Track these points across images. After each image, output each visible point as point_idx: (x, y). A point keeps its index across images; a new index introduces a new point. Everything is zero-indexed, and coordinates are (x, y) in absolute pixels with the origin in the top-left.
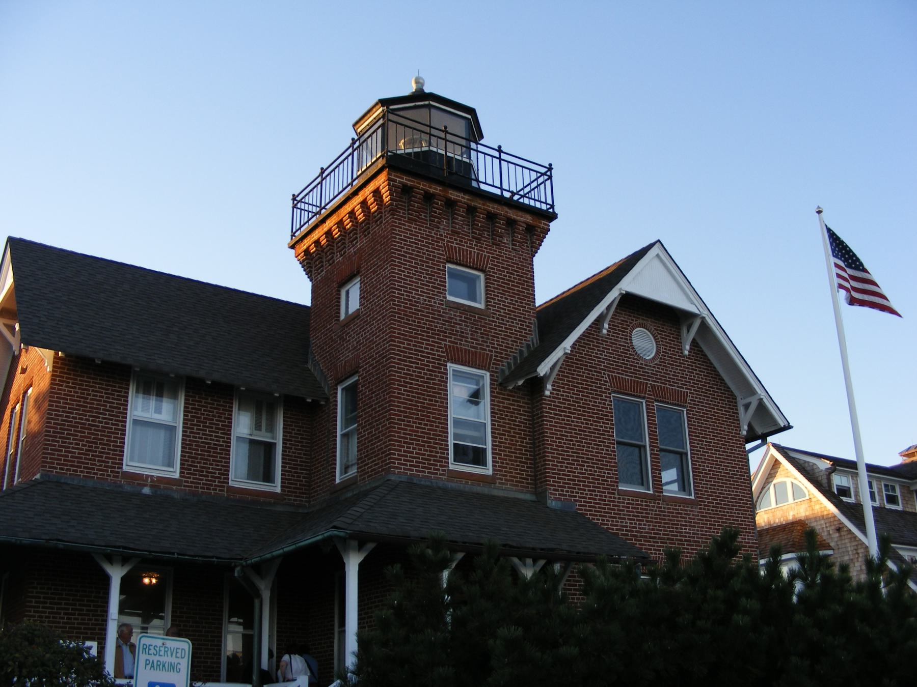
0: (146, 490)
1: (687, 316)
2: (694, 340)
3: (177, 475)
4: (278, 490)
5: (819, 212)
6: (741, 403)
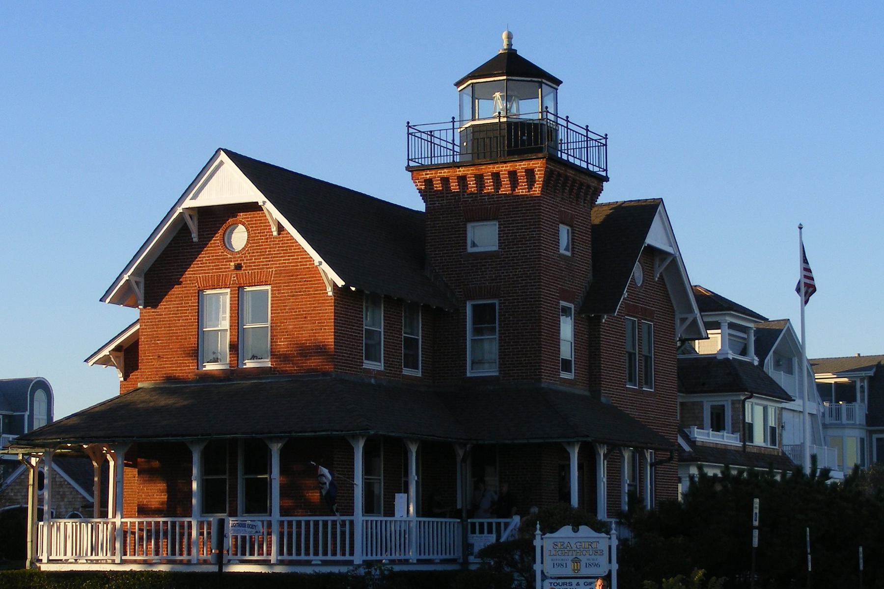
0: (373, 381)
1: (668, 254)
3: (382, 368)
4: (420, 375)
5: (800, 228)
6: (678, 316)
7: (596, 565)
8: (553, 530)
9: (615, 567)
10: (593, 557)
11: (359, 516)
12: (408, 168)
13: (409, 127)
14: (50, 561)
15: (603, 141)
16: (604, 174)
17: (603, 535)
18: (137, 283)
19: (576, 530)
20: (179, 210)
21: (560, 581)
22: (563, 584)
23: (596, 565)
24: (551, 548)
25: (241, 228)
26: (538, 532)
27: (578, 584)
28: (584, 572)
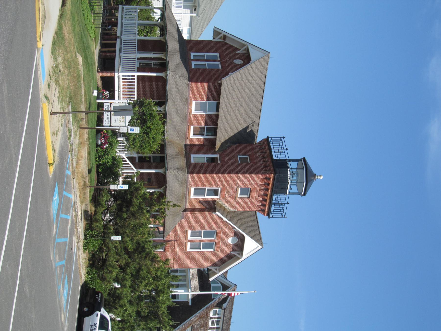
2: (235, 256)
6: (218, 268)
11: (136, 74)
12: (268, 137)
13: (283, 137)
14: (123, 8)
15: (283, 216)
16: (271, 216)
18: (220, 38)
27: (108, 115)
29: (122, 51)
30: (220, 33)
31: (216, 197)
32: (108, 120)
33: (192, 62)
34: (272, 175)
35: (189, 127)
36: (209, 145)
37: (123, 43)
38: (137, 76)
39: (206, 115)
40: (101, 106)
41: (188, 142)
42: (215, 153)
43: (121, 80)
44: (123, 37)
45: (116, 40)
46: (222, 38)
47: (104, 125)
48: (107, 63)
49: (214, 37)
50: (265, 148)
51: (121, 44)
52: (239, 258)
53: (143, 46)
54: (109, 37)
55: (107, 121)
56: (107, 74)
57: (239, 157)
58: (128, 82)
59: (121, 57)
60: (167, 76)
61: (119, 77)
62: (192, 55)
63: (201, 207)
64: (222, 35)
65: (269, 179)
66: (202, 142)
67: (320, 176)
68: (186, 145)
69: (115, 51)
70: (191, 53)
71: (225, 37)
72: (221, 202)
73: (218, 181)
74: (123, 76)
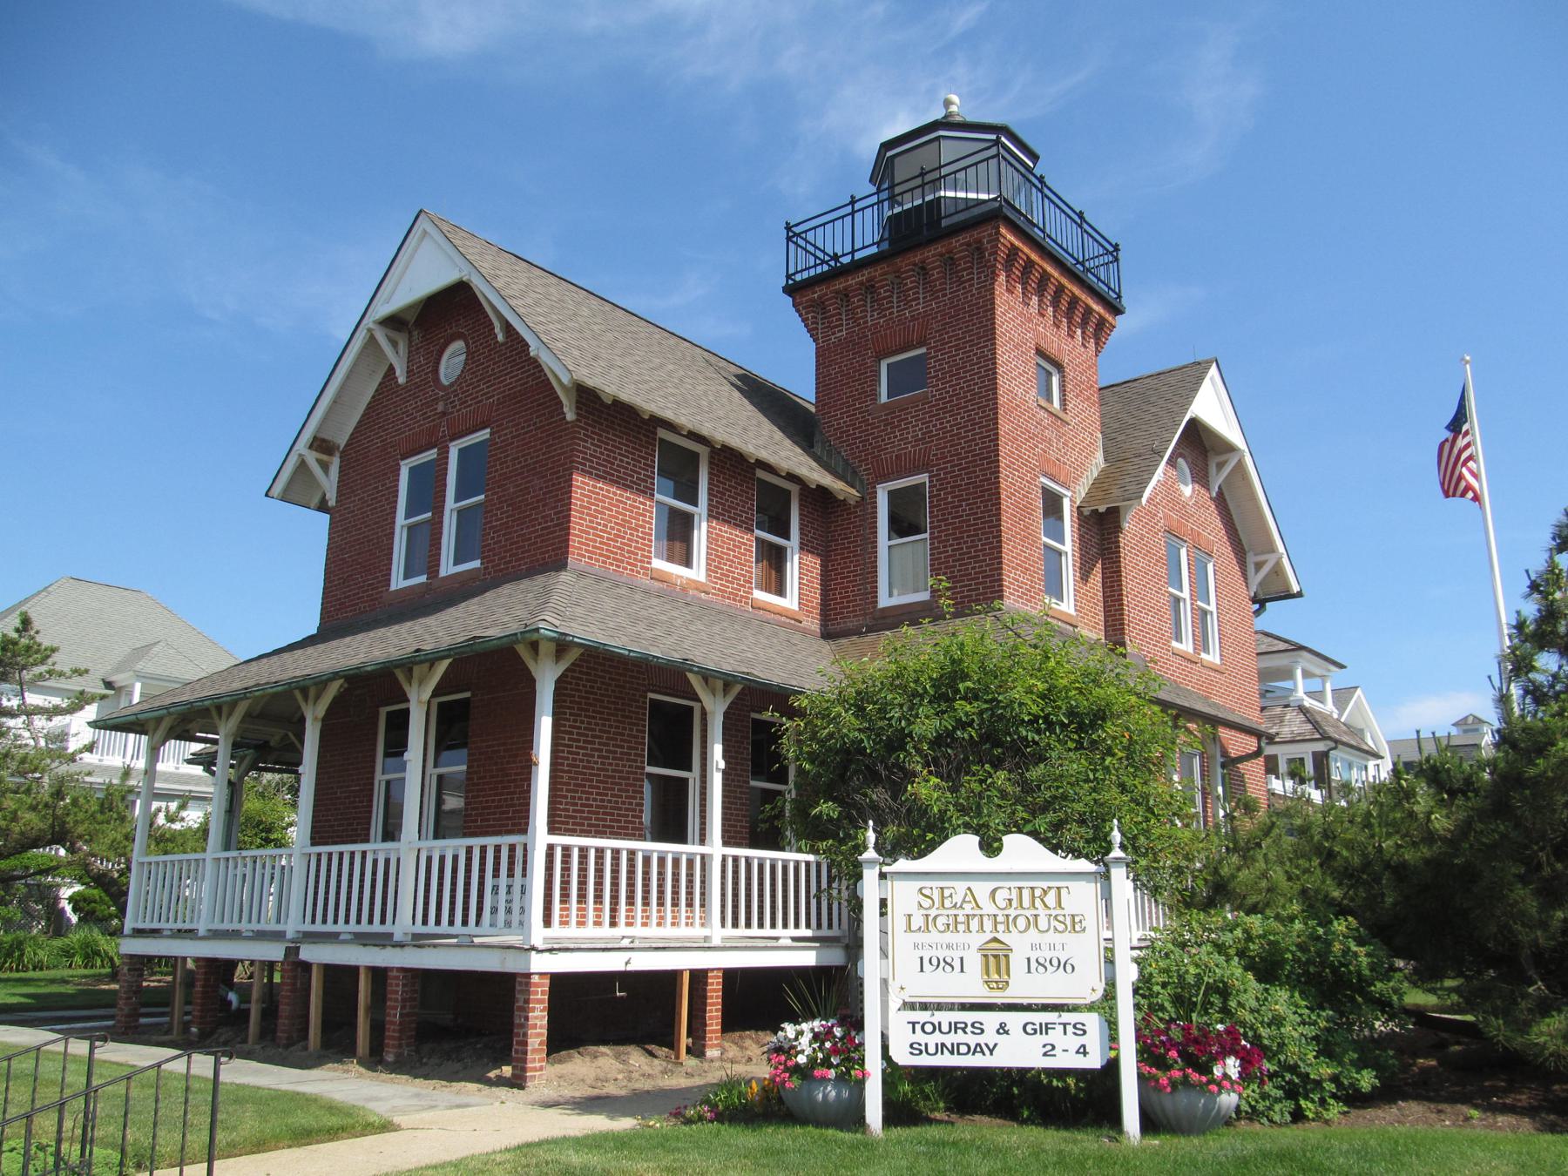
7: (1063, 965)
8: (920, 846)
9: (1128, 974)
10: (1052, 937)
11: (541, 836)
13: (788, 228)
14: (138, 933)
17: (1084, 865)
18: (325, 467)
19: (990, 847)
20: (369, 322)
21: (945, 1017)
22: (954, 1027)
23: (1063, 965)
24: (913, 909)
25: (458, 345)
26: (871, 854)
27: (1003, 1029)
28: (1022, 987)
29: (377, 927)
30: (302, 465)
31: (1066, 503)
32: (1046, 1028)
33: (443, 573)
34: (1003, 231)
35: (757, 607)
36: (835, 530)
37: (330, 927)
38: (553, 829)
39: (710, 516)
40: (927, 1095)
41: (813, 624)
42: (868, 501)
43: (556, 930)
44: (293, 925)
45: (307, 966)
46: (325, 457)
47: (1094, 1061)
48: (461, 1025)
49: (316, 500)
50: (845, 295)
51: (333, 937)
52: (1240, 465)
53: (345, 815)
54: (285, 1009)
55: (1055, 1036)
56: (538, 1019)
57: (884, 398)
58: (565, 896)
59: (416, 936)
60: (562, 645)
61: (563, 943)
62: (398, 582)
63: (1097, 577)
64: (312, 458)
65: (1014, 251)
66: (814, 562)
67: (947, 103)
68: (827, 635)
69: (379, 975)
70: (393, 587)
71: (321, 445)
72: (1082, 490)
73: (1018, 485)
74: (547, 922)
